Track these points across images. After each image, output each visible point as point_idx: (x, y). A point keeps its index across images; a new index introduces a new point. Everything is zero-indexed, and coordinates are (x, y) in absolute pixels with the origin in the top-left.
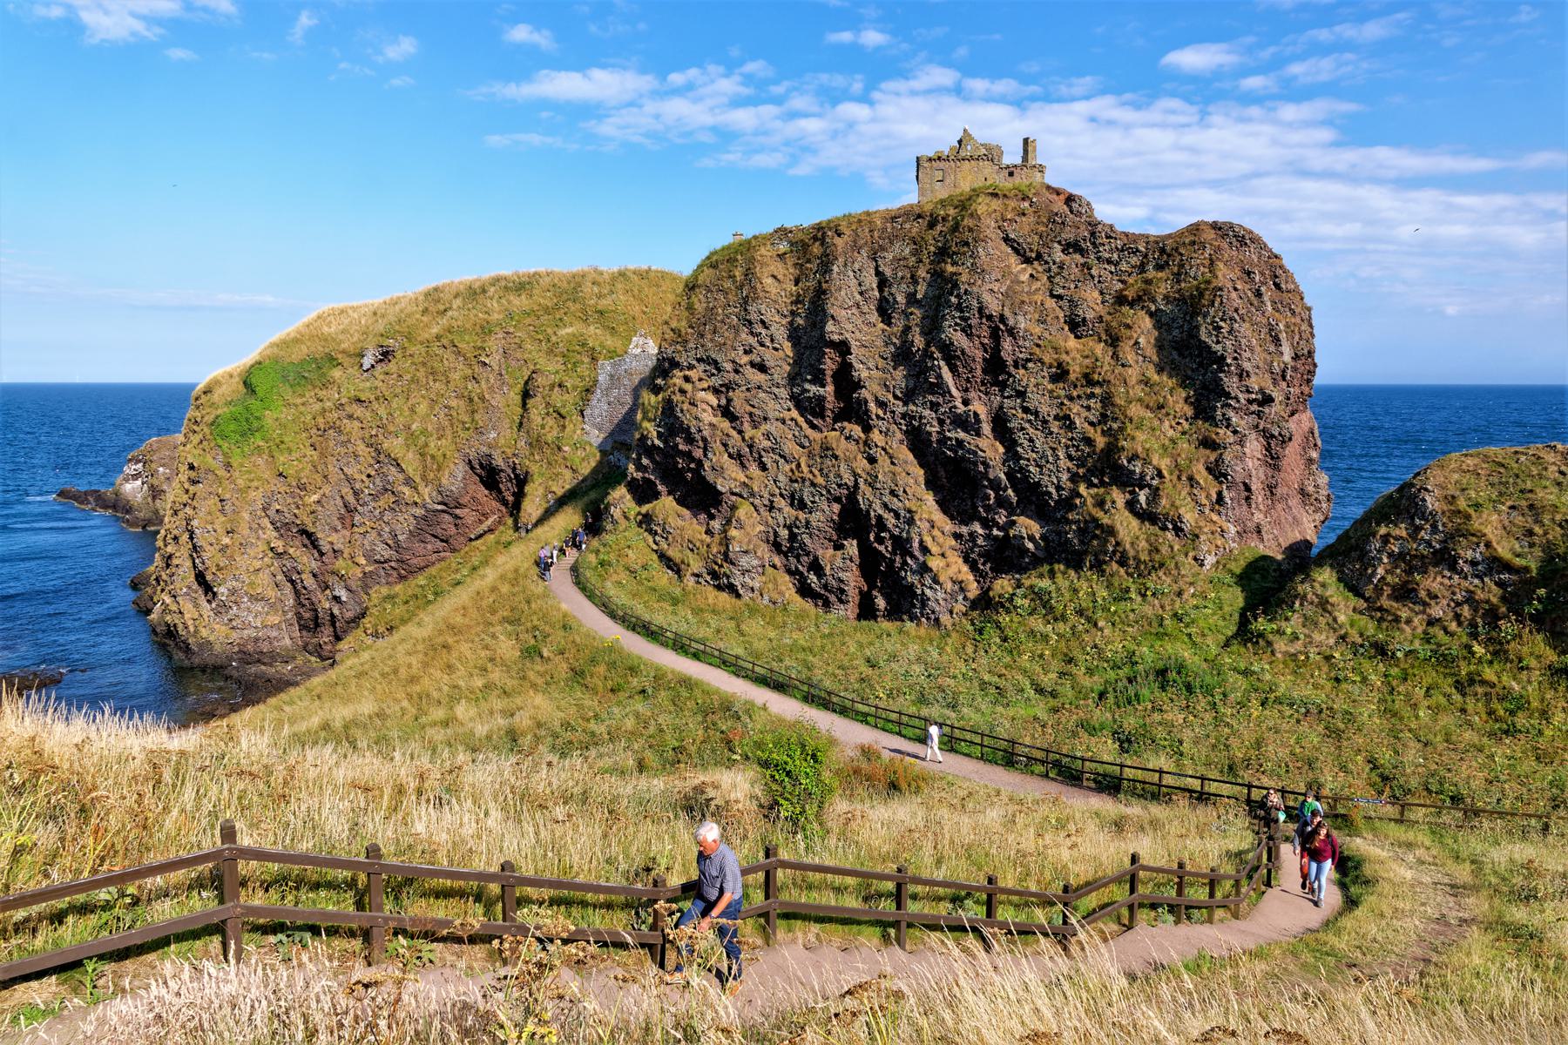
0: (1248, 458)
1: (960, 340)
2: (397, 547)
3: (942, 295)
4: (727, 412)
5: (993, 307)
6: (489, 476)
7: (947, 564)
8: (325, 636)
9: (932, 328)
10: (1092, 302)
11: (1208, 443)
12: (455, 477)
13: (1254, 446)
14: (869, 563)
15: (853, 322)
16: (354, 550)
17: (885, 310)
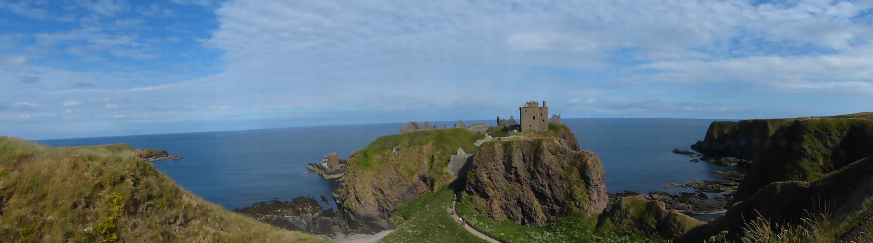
0: (595, 196)
1: (541, 170)
2: (403, 195)
3: (537, 160)
4: (490, 178)
5: (547, 164)
6: (424, 179)
8: (386, 214)
9: (535, 166)
10: (566, 164)
11: (588, 193)
12: (416, 178)
13: (596, 193)
15: (518, 162)
17: (524, 160)
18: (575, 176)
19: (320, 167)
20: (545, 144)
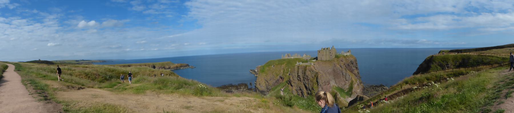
12: (278, 77)
16: (271, 82)
18: (315, 81)
19: (255, 71)
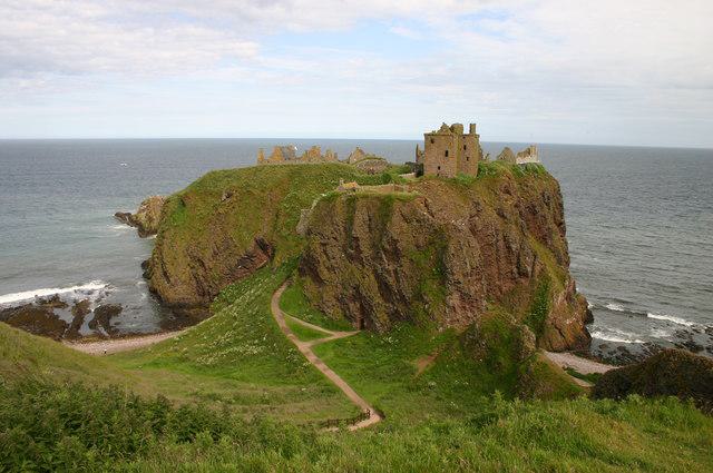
7: (381, 316)
12: (251, 246)
14: (362, 309)
15: (360, 230)
20: (396, 205)
